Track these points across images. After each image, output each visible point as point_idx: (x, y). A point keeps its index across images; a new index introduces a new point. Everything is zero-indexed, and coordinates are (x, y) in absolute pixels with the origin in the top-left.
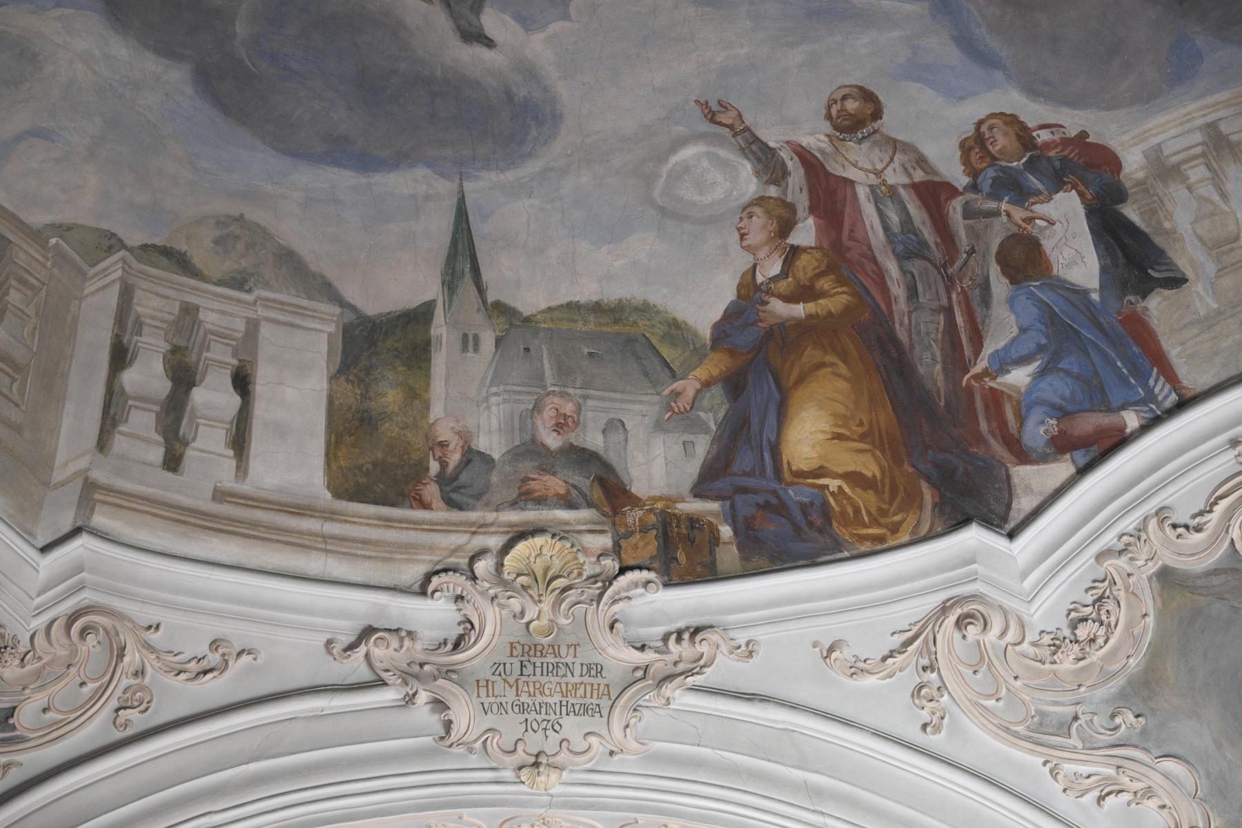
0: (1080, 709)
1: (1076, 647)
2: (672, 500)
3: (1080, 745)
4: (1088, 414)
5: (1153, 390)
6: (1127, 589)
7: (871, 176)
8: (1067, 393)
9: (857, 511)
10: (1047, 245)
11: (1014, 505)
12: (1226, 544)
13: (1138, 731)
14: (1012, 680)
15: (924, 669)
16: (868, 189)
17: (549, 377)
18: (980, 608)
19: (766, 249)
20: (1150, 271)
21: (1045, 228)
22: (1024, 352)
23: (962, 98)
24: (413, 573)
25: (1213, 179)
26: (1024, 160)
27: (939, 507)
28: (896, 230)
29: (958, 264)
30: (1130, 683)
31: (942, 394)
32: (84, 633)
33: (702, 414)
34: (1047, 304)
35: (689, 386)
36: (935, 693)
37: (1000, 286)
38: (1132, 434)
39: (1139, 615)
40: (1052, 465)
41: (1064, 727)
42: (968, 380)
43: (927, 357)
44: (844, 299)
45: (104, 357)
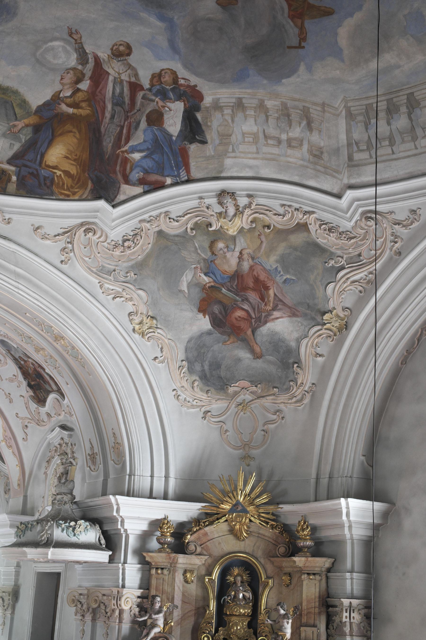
0: (117, 268)
1: (122, 248)
3: (113, 279)
4: (155, 175)
5: (180, 174)
6: (146, 234)
7: (117, 74)
8: (151, 166)
9: (63, 184)
10: (166, 116)
11: (118, 197)
12: (184, 228)
13: (133, 279)
14: (97, 254)
15: (68, 243)
16: (113, 78)
18: (95, 227)
19: (68, 86)
20: (197, 136)
21: (168, 111)
22: (142, 148)
23: (161, 60)
25: (232, 115)
26: (172, 87)
27: (92, 191)
28: (117, 94)
29: (133, 113)
30: (136, 263)
31: (108, 153)
33: (21, 136)
34: (157, 136)
35: (20, 124)
36: (69, 251)
37: (143, 124)
38: (167, 185)
39: (147, 243)
40: (136, 188)
41: (109, 273)
42: (119, 152)
43: (108, 140)
44: (88, 112)
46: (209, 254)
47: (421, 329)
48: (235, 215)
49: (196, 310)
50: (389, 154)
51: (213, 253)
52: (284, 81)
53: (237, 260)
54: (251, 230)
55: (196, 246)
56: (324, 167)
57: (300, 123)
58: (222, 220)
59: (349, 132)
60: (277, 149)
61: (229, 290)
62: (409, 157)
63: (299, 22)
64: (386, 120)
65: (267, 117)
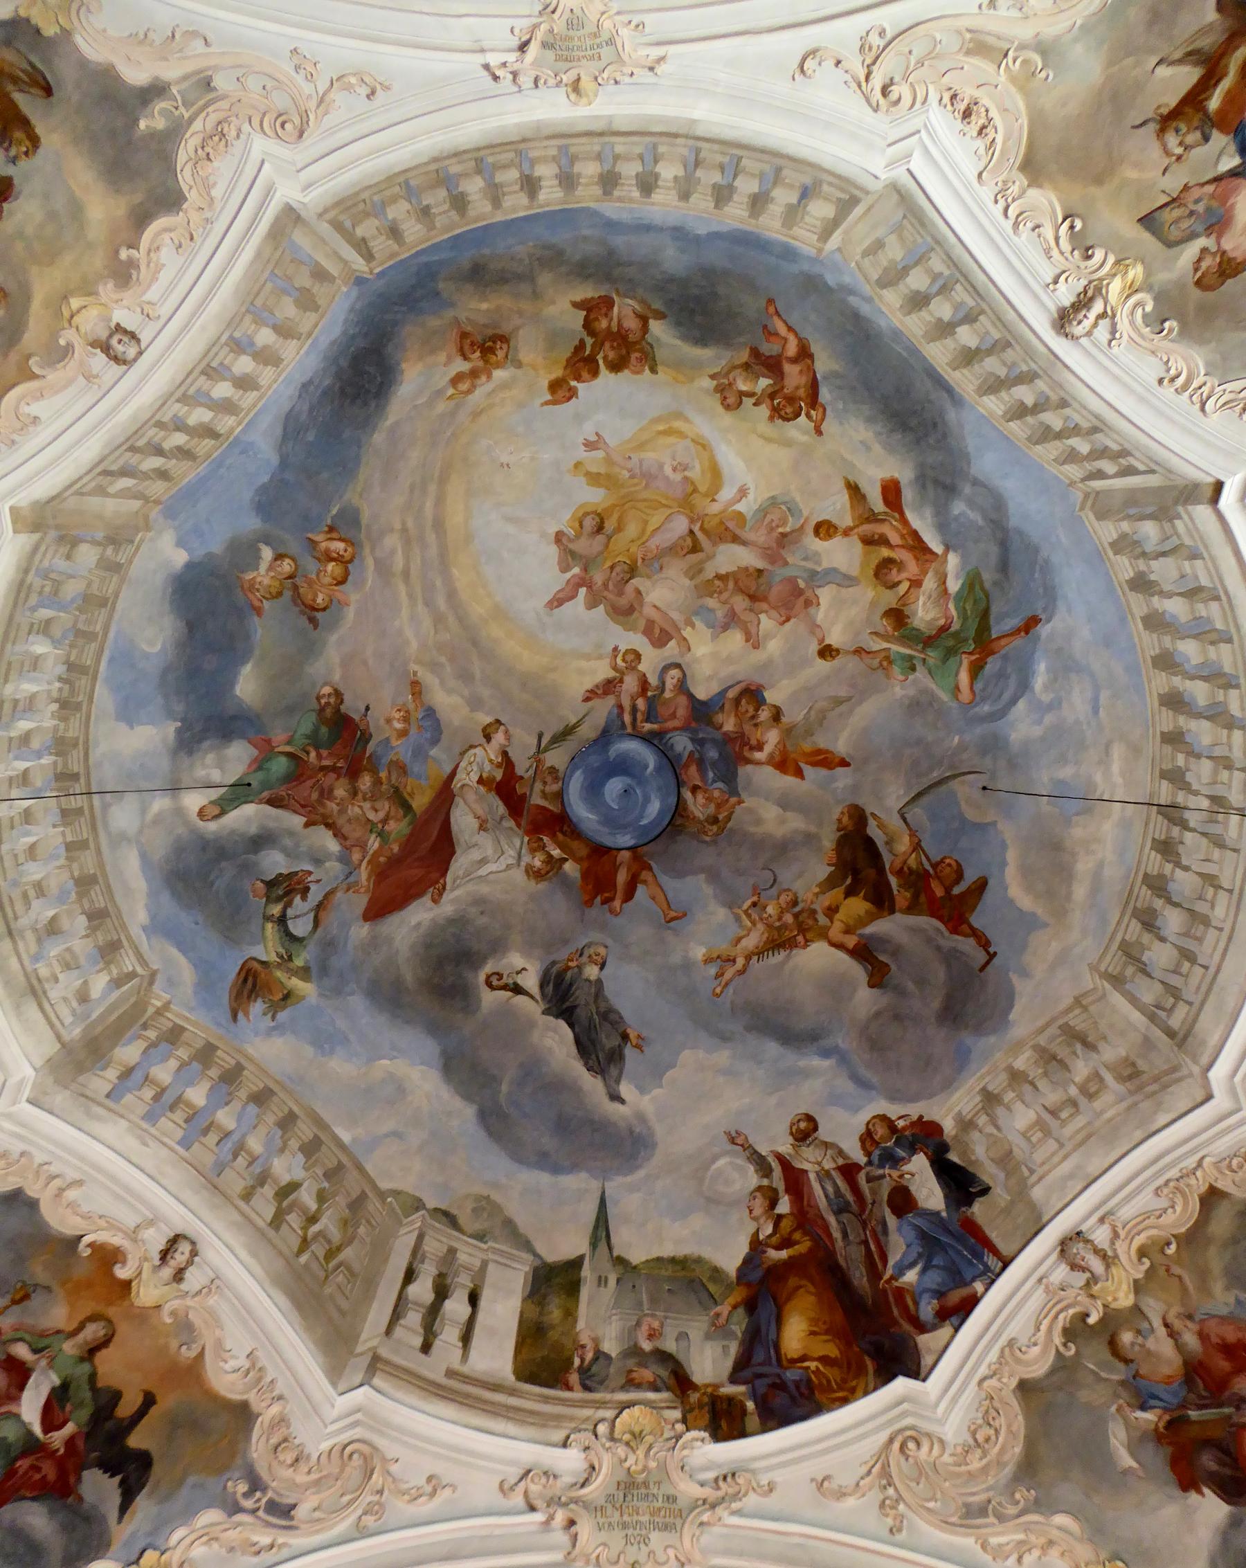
2: (716, 1386)
3: (996, 1521)
9: (829, 1381)
10: (913, 1189)
11: (923, 1363)
12: (1053, 1352)
17: (646, 1306)
22: (911, 1260)
24: (559, 1436)
28: (832, 1196)
32: (351, 1456)
33: (733, 1327)
35: (724, 1309)
37: (891, 1221)
43: (857, 1274)
45: (401, 1276)
46: (1121, 1366)
48: (1108, 1267)
49: (1177, 1493)
50: (1204, 976)
51: (1127, 1361)
52: (1011, 1017)
53: (1170, 1342)
54: (1150, 1273)
55: (1092, 1371)
57: (1075, 1053)
58: (1096, 1289)
59: (1134, 1001)
60: (1080, 1117)
61: (1200, 1407)
62: (1226, 950)
63: (964, 927)
65: (1032, 1084)
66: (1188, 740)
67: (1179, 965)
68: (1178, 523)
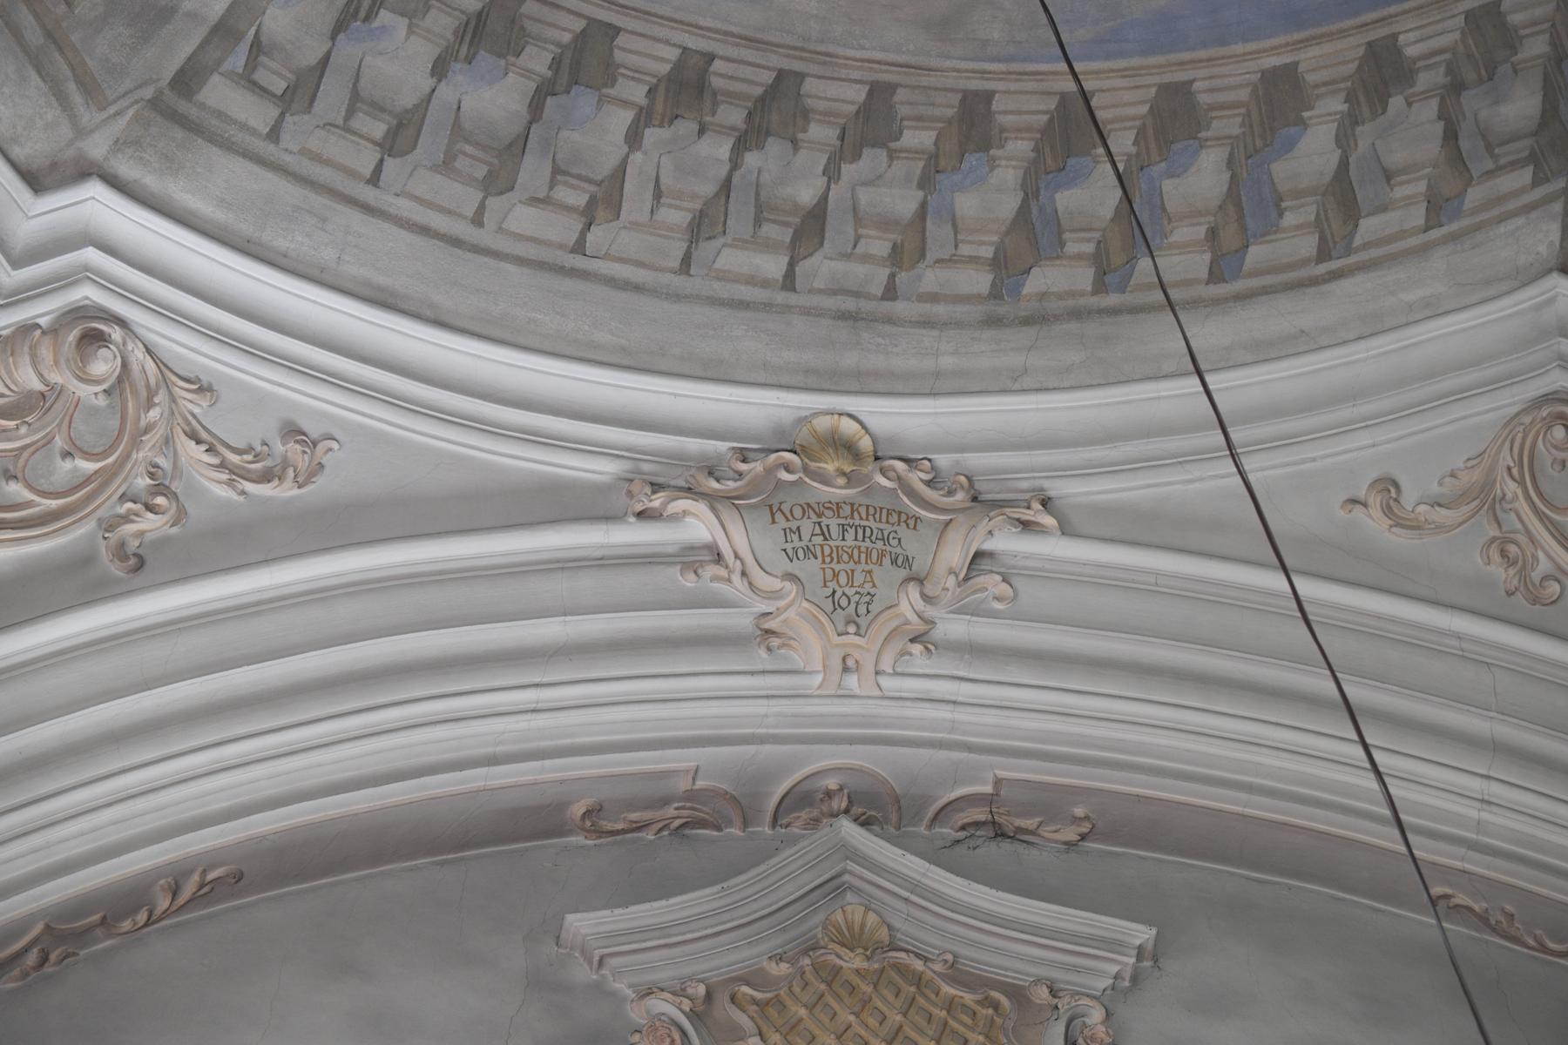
47: (48, 927)
56: (49, 35)
62: (425, 231)
64: (438, 51)
66: (971, 160)
67: (377, 108)
68: (1526, 175)
